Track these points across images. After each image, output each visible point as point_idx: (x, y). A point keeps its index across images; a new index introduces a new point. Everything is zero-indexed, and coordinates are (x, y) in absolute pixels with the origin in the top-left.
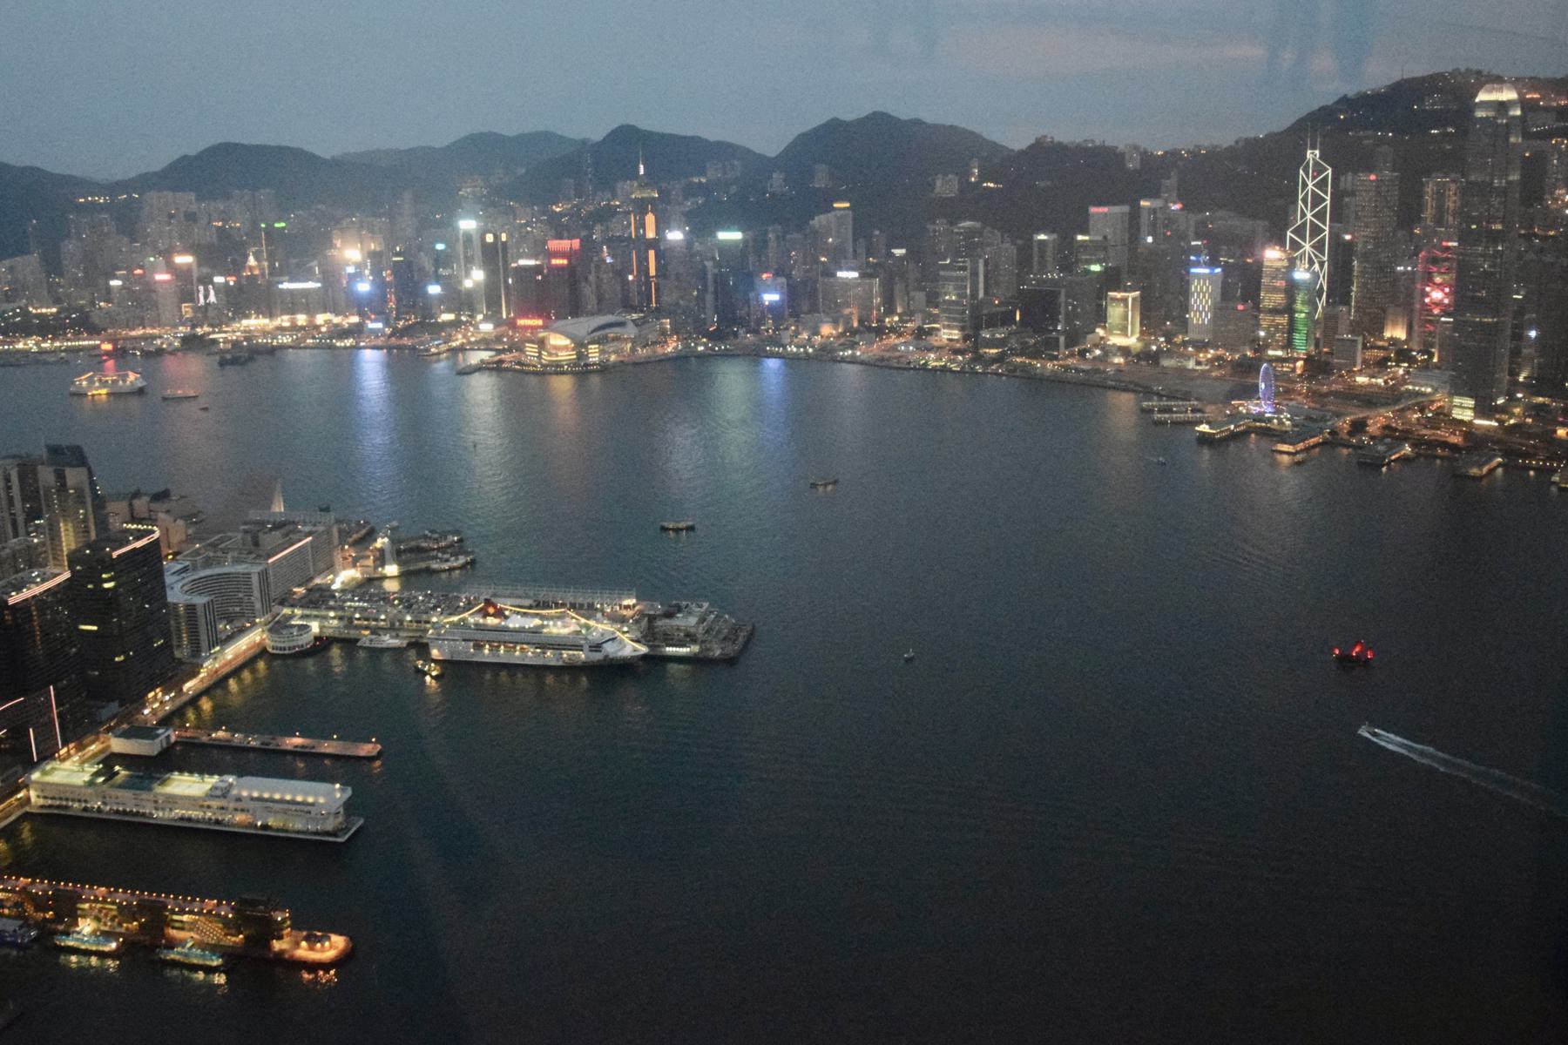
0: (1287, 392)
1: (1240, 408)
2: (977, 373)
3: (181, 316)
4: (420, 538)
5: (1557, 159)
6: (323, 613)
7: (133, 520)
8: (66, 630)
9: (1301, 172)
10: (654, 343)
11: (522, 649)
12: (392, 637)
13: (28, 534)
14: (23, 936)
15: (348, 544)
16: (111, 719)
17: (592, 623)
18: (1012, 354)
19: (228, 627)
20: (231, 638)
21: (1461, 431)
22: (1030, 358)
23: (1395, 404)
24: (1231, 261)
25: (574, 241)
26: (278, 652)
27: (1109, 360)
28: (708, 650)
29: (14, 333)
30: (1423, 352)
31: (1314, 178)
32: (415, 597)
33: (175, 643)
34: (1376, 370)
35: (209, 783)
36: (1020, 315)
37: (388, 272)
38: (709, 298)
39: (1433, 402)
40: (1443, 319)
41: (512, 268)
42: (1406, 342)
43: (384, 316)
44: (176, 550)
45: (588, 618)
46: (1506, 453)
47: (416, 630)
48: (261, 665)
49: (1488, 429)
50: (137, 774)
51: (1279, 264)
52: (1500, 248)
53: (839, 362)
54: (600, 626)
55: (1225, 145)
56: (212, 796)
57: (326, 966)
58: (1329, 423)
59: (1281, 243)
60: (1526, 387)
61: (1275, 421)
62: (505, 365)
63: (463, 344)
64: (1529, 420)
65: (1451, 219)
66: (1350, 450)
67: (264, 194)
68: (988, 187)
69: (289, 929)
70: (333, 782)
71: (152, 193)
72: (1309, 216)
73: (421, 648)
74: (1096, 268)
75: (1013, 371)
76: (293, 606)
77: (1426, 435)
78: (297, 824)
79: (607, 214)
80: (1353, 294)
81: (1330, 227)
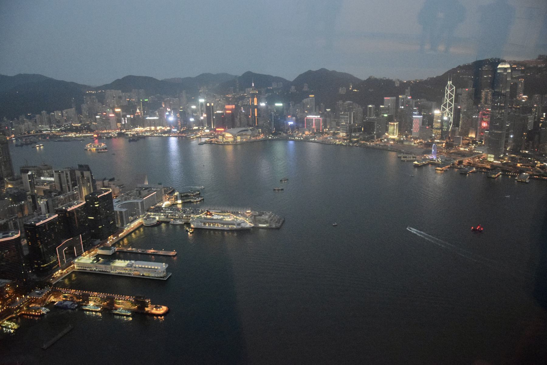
0: (440, 152)
1: (427, 157)
2: (350, 146)
3: (117, 127)
4: (188, 192)
5: (521, 85)
6: (160, 214)
7: (104, 187)
8: (84, 218)
9: (446, 88)
10: (256, 136)
11: (217, 225)
12: (180, 221)
13: (73, 191)
14: (73, 306)
15: (167, 194)
16: (98, 244)
17: (238, 217)
18: (361, 140)
19: (132, 218)
20: (133, 221)
21: (490, 164)
22: (366, 141)
23: (471, 156)
24: (425, 114)
25: (233, 106)
26: (146, 225)
27: (389, 142)
28: (271, 225)
29: (68, 131)
30: (479, 141)
31: (450, 90)
32: (186, 209)
33: (116, 222)
34: (466, 146)
35: (127, 263)
36: (363, 129)
37: (178, 114)
38: (273, 123)
39: (482, 156)
40: (486, 132)
41: (215, 114)
42: (475, 138)
43: (176, 127)
44: (116, 195)
45: (237, 216)
46: (503, 171)
47: (187, 219)
48: (142, 230)
49: (498, 164)
50: (106, 260)
51: (439, 115)
52: (503, 111)
53: (311, 142)
54: (240, 218)
55: (425, 79)
56: (128, 267)
57: (161, 315)
58: (452, 161)
59: (440, 108)
60: (508, 152)
61: (436, 161)
62: (213, 142)
63: (200, 136)
64: (510, 161)
65: (489, 102)
66: (458, 169)
67: (141, 91)
68: (355, 91)
69: (150, 305)
70: (163, 263)
71: (108, 90)
72: (448, 101)
73: (188, 224)
74: (386, 115)
75: (361, 146)
76: (151, 212)
77: (479, 165)
78: (152, 275)
79: (243, 98)
80: (460, 124)
81: (454, 104)
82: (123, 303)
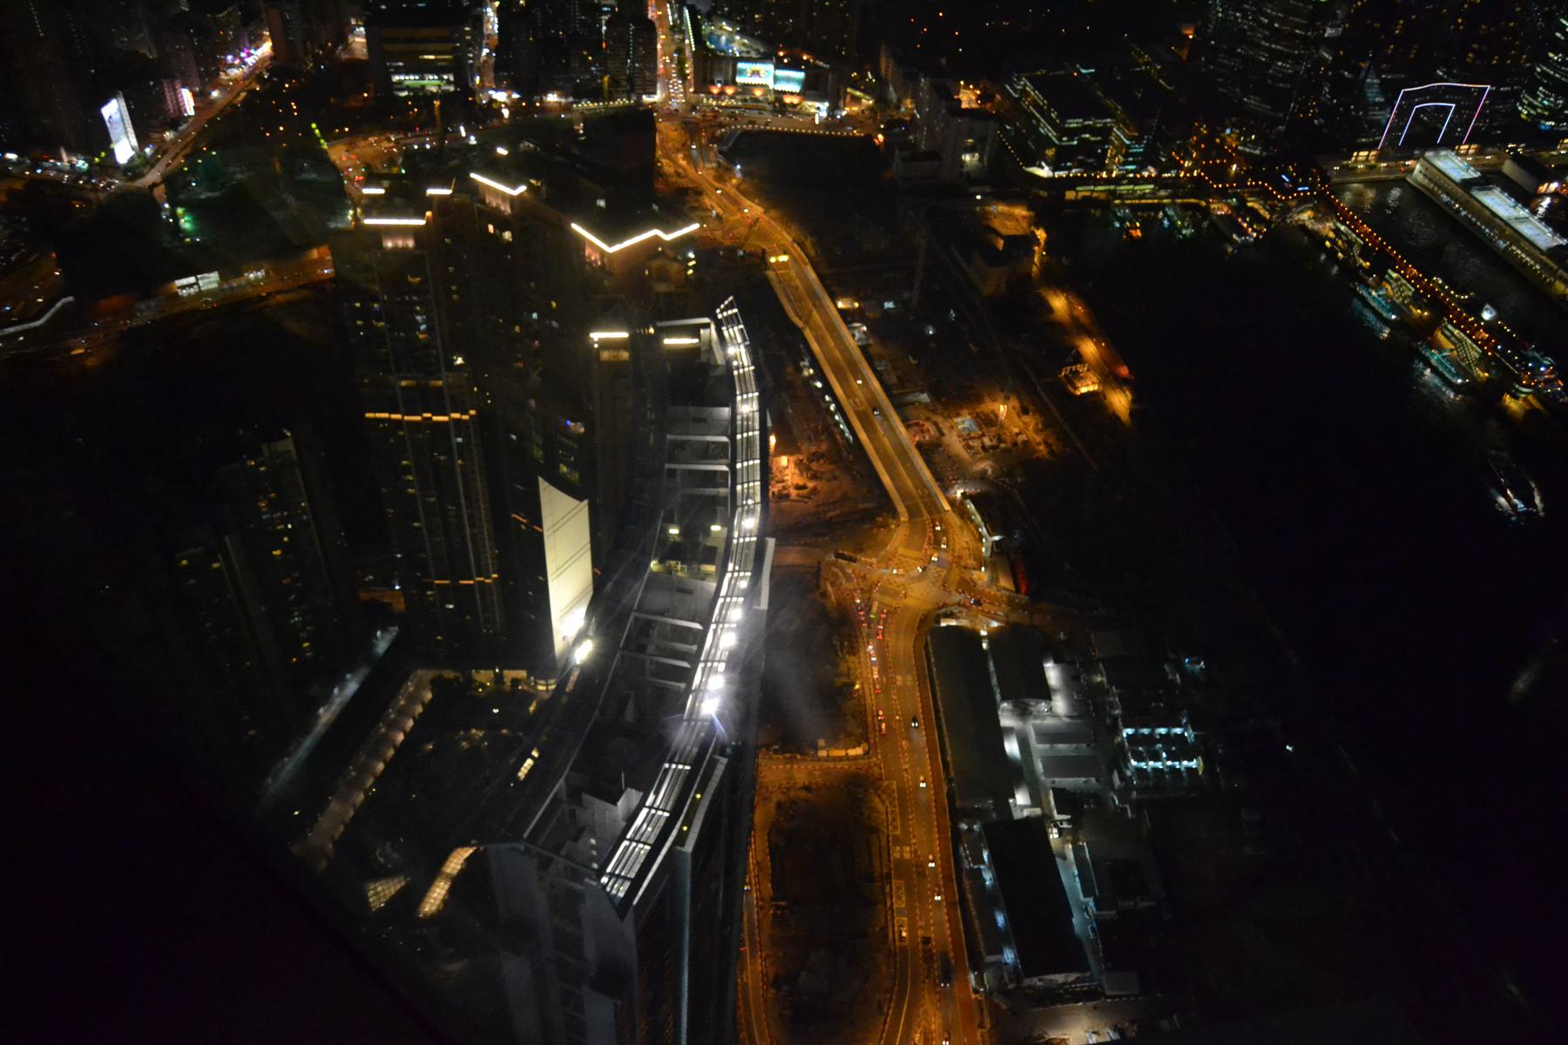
35: (1557, 241)
82: (1460, 341)
